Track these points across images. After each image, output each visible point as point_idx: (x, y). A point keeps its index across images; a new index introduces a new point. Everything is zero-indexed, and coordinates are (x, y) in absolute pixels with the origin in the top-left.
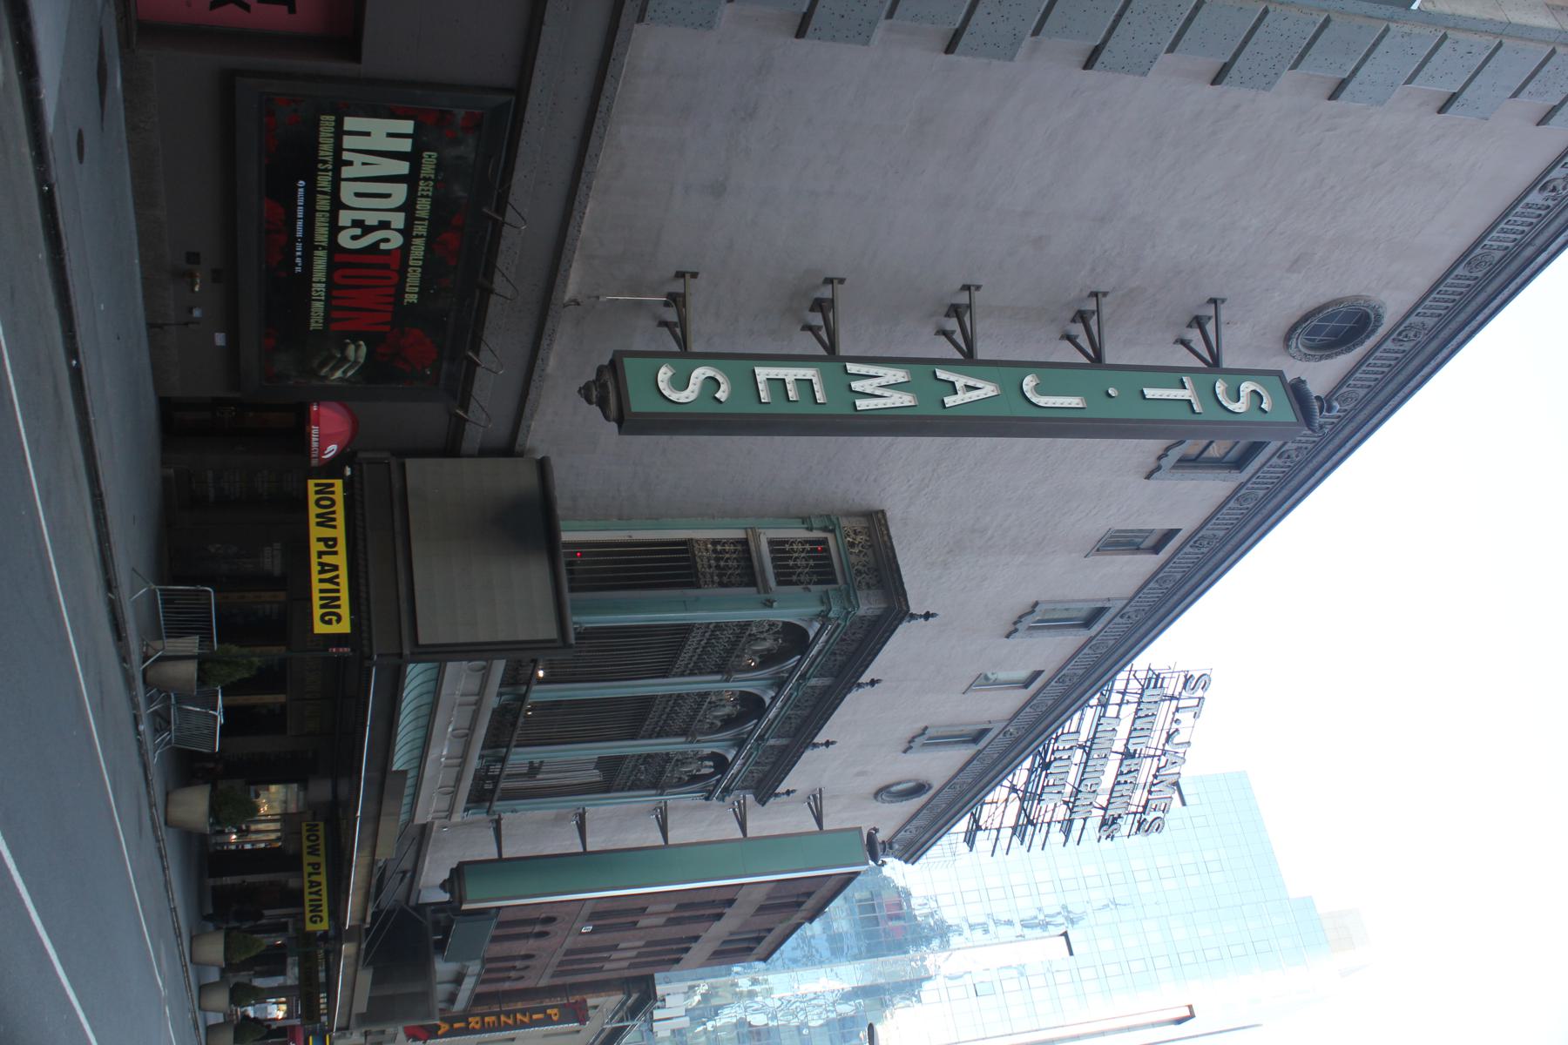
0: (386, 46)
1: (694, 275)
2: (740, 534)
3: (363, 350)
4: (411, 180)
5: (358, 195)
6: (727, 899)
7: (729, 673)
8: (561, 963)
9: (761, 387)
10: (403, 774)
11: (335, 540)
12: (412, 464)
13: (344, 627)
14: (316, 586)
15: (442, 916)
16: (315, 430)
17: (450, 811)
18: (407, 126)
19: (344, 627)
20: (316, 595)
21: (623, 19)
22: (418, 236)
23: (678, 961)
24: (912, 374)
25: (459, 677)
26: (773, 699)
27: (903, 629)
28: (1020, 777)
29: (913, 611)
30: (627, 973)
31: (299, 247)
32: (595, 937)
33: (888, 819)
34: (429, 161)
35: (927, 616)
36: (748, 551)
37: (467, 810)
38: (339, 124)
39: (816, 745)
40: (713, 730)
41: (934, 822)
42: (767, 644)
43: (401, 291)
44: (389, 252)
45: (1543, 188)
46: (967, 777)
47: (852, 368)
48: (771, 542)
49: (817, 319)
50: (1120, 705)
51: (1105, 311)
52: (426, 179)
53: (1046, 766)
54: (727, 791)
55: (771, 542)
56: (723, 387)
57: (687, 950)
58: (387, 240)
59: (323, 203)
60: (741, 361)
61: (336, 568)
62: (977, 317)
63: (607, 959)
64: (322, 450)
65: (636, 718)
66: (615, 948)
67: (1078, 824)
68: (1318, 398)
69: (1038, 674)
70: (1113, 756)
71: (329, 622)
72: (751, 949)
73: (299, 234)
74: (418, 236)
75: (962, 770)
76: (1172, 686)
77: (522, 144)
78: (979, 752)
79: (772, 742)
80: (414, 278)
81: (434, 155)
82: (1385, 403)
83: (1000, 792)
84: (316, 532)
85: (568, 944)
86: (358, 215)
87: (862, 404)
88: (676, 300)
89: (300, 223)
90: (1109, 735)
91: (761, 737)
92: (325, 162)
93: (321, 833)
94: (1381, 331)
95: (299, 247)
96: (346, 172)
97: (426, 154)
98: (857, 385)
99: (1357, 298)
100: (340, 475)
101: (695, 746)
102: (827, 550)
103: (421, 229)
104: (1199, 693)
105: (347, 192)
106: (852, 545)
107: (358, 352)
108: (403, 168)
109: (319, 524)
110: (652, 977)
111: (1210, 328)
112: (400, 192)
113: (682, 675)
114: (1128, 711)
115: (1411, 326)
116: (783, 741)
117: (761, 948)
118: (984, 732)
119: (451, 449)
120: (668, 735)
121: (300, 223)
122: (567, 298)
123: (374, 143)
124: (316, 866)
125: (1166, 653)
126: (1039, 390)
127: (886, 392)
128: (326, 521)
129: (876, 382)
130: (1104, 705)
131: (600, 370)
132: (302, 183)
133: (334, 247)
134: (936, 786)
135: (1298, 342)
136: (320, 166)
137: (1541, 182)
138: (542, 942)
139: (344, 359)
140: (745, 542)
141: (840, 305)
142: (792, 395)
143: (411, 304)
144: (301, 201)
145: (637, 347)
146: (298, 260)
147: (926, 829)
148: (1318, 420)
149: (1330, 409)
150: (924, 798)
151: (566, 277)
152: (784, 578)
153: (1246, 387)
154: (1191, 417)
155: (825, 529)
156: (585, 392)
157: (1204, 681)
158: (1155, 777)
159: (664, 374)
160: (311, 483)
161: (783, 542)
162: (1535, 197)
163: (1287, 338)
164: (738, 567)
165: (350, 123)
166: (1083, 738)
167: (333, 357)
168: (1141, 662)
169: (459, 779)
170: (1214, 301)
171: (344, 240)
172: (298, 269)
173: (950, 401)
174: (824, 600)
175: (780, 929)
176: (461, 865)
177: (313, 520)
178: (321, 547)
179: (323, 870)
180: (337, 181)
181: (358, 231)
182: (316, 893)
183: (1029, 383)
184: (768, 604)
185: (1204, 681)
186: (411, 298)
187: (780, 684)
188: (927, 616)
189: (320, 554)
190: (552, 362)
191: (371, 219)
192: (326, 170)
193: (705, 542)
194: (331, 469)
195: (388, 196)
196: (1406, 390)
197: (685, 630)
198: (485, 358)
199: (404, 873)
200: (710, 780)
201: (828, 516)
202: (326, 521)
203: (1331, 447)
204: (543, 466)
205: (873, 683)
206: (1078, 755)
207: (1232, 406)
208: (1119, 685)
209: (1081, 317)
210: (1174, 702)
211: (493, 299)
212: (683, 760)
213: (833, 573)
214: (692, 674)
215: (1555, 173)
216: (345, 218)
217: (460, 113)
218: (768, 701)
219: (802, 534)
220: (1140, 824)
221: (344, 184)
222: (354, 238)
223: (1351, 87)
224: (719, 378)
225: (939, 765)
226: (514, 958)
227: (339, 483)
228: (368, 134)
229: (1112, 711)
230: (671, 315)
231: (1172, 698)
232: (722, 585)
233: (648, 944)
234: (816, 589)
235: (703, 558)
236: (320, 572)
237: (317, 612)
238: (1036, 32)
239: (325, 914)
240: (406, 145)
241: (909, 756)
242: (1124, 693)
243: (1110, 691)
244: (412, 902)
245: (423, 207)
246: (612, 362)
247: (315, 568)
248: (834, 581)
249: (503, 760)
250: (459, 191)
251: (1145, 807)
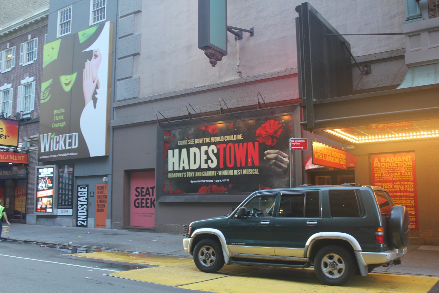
0: (149, 162)
3: (269, 151)
4: (188, 147)
5: (195, 163)
18: (170, 152)
22: (210, 140)
38: (171, 172)
43: (238, 141)
44: (218, 150)
52: (188, 142)
58: (213, 151)
59: (199, 174)
73: (212, 181)
74: (210, 140)
77: (171, 117)
80: (230, 138)
81: (179, 142)
89: (207, 181)
92: (184, 175)
96: (187, 168)
97: (179, 144)
103: (207, 140)
107: (271, 154)
108: (184, 151)
121: (207, 181)
123: (176, 161)
132: (191, 182)
133: (217, 168)
136: (185, 176)
139: (276, 158)
143: (242, 137)
144: (199, 181)
146: (224, 181)
151: (228, 82)
165: (170, 169)
167: (275, 163)
171: (213, 165)
172: (228, 180)
180: (190, 171)
181: (209, 161)
186: (240, 137)
191: (204, 157)
192: (186, 174)
195: (195, 153)
216: (204, 166)
217: (165, 137)
221: (191, 168)
222: (212, 162)
228: (173, 163)
240: (176, 151)
245: (199, 141)
250: (192, 131)
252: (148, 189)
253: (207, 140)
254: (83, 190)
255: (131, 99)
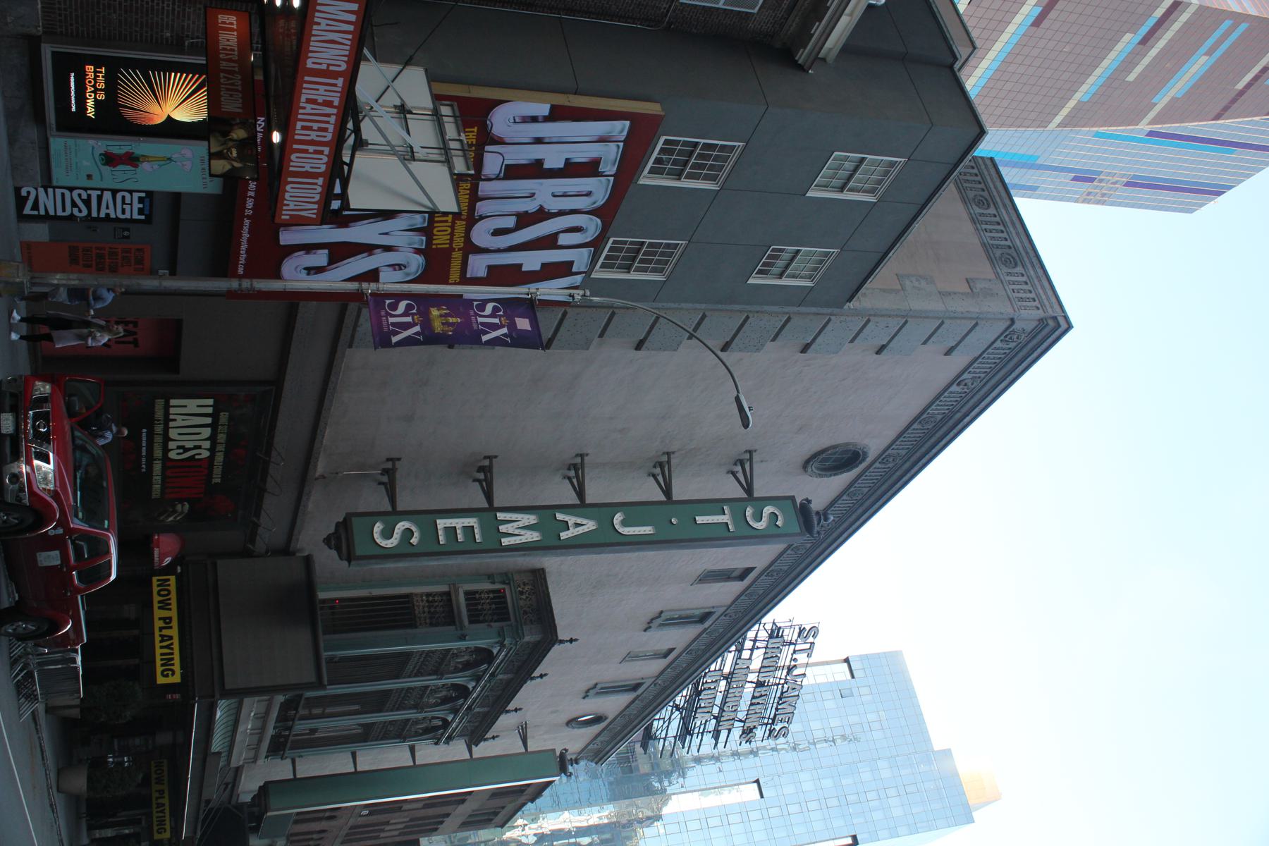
1: (399, 459)
2: (444, 588)
3: (187, 506)
6: (461, 799)
7: (442, 675)
8: (347, 835)
9: (440, 533)
10: (219, 753)
11: (170, 618)
12: (220, 563)
13: (176, 679)
14: (158, 651)
15: (255, 809)
16: (156, 551)
17: (255, 759)
18: (211, 402)
19: (176, 679)
20: (158, 658)
21: (339, 348)
23: (436, 829)
24: (540, 518)
25: (252, 707)
26: (474, 688)
27: (557, 648)
28: (679, 700)
29: (560, 638)
30: (398, 839)
31: (144, 460)
32: (371, 818)
33: (575, 741)
34: (224, 417)
35: (571, 641)
36: (450, 600)
37: (267, 757)
39: (508, 712)
40: (457, 670)
41: (613, 738)
42: (466, 658)
43: (210, 475)
45: (958, 384)
46: (633, 710)
47: (501, 516)
48: (467, 593)
49: (481, 476)
50: (752, 650)
51: (673, 462)
53: (698, 693)
54: (450, 738)
55: (467, 593)
56: (416, 534)
57: (442, 823)
60: (427, 517)
61: (171, 638)
62: (586, 470)
63: (383, 831)
64: (161, 561)
65: (380, 702)
66: (388, 823)
67: (723, 734)
68: (818, 513)
69: (671, 650)
70: (748, 685)
71: (167, 676)
72: (491, 820)
75: (628, 707)
76: (789, 635)
78: (638, 697)
79: (477, 710)
82: (881, 496)
83: (665, 712)
84: (158, 613)
85: (350, 824)
86: (180, 444)
87: (506, 541)
88: (390, 473)
90: (744, 671)
91: (493, 675)
93: (165, 768)
94: (869, 460)
95: (144, 460)
96: (172, 424)
98: (503, 528)
99: (847, 444)
100: (174, 573)
101: (444, 681)
102: (504, 597)
103: (221, 448)
104: (811, 639)
105: (173, 433)
106: (521, 593)
108: (209, 420)
109: (160, 608)
110: (417, 842)
111: (747, 466)
112: (207, 432)
113: (409, 676)
114: (759, 654)
115: (889, 456)
116: (485, 709)
117: (499, 819)
118: (671, 650)
119: (247, 554)
120: (404, 709)
122: (317, 474)
124: (161, 792)
125: (789, 611)
126: (625, 523)
127: (522, 532)
128: (165, 605)
129: (515, 524)
130: (740, 651)
131: (338, 525)
133: (165, 458)
134: (611, 717)
135: (813, 467)
137: (957, 380)
138: (333, 823)
139: (174, 511)
140: (448, 594)
141: (495, 470)
142: (460, 537)
145: (361, 509)
147: (609, 743)
148: (816, 529)
149: (826, 520)
150: (603, 725)
151: (315, 467)
152: (475, 618)
153: (768, 510)
154: (728, 535)
155: (504, 583)
156: (327, 541)
157: (814, 631)
158: (780, 698)
159: (378, 528)
160: (155, 579)
161: (475, 592)
162: (954, 388)
163: (806, 465)
164: (442, 612)
165: (173, 402)
166: (727, 670)
168: (768, 619)
169: (260, 741)
170: (750, 452)
173: (564, 535)
174: (501, 634)
175: (510, 807)
176: (267, 784)
177: (156, 605)
178: (161, 624)
179: (166, 795)
180: (166, 429)
182: (162, 812)
183: (618, 518)
184: (463, 638)
185: (814, 631)
187: (478, 679)
188: (571, 641)
189: (161, 629)
190: (310, 506)
191: (189, 445)
193: (421, 595)
194: (169, 570)
196: (894, 489)
197: (408, 655)
198: (264, 520)
199: (227, 784)
200: (437, 732)
201: (506, 574)
202: (165, 605)
203: (851, 520)
204: (308, 560)
205: (541, 676)
206: (723, 683)
207: (755, 525)
208: (751, 634)
209: (661, 465)
210: (792, 647)
211: (266, 495)
212: (417, 722)
213: (508, 613)
214: (416, 676)
215: (966, 376)
216: (172, 445)
218: (495, 651)
219: (487, 586)
220: (771, 731)
223: (813, 346)
224: (414, 528)
225: (612, 705)
226: (312, 833)
227: (173, 579)
229: (746, 654)
230: (385, 479)
231: (791, 643)
232: (431, 625)
233: (411, 820)
234: (496, 625)
235: (420, 606)
236: (162, 641)
237: (159, 669)
238: (601, 336)
239: (168, 827)
240: (210, 410)
241: (586, 700)
242: (755, 641)
243: (744, 639)
244: (233, 802)
245: (222, 438)
246: (345, 519)
247: (158, 639)
248: (508, 619)
249: (290, 729)
251: (774, 720)
252: (135, 333)
253: (221, 448)
254: (137, 206)
255: (353, 336)
